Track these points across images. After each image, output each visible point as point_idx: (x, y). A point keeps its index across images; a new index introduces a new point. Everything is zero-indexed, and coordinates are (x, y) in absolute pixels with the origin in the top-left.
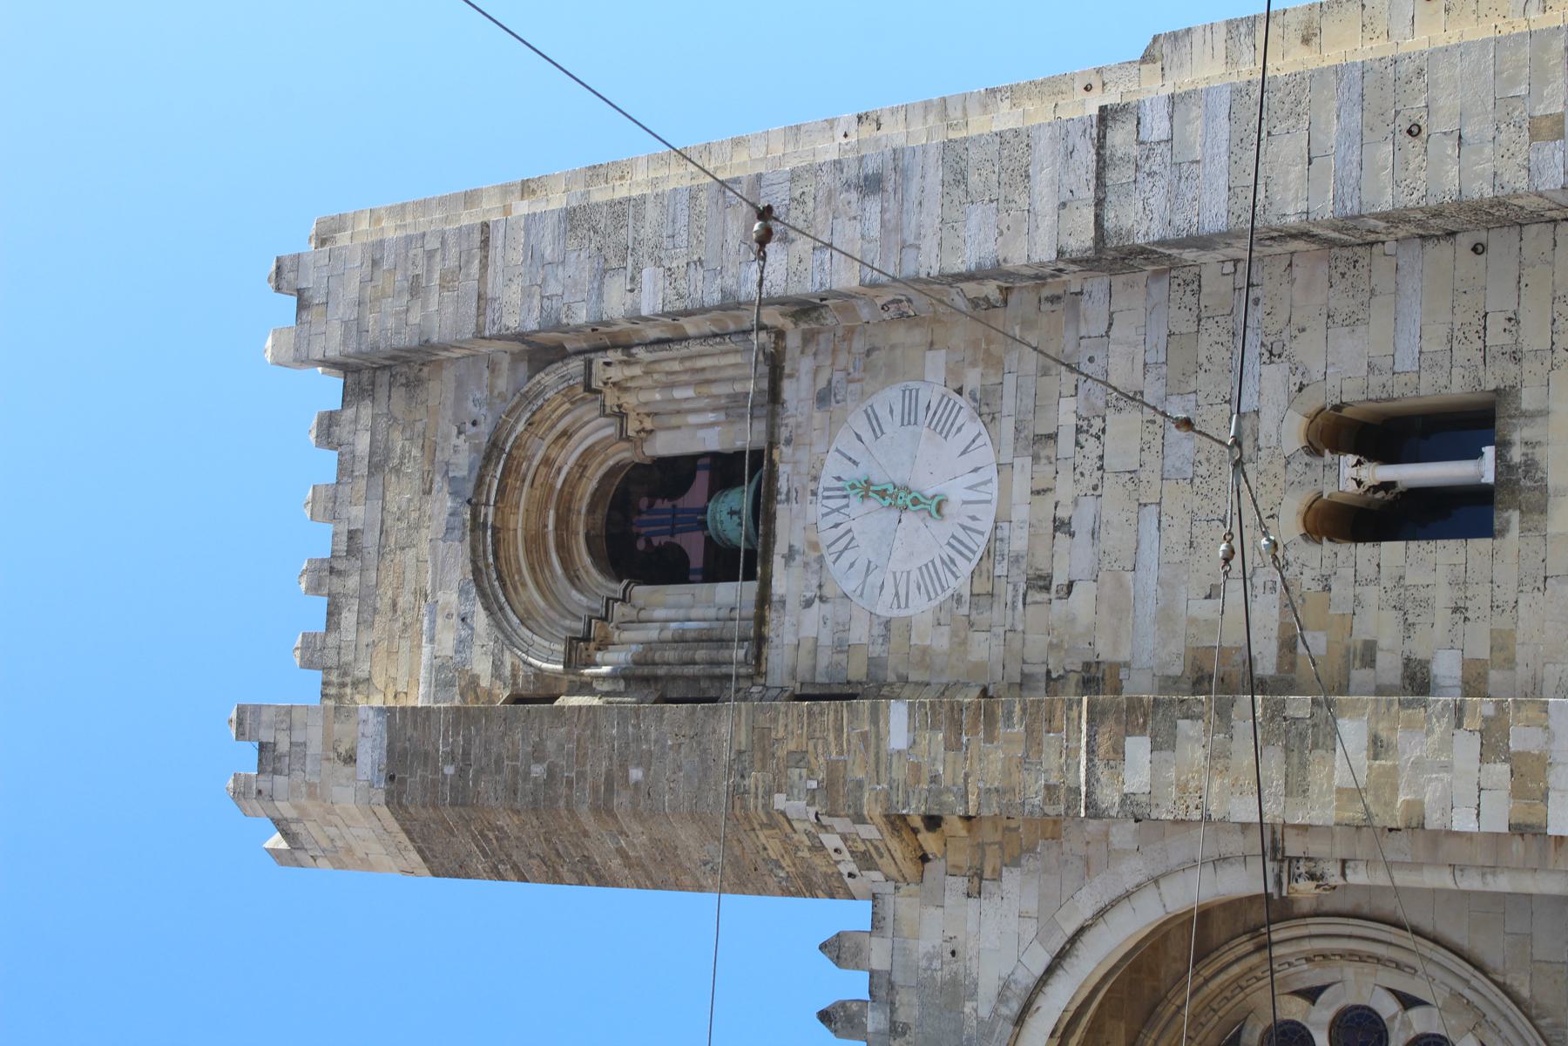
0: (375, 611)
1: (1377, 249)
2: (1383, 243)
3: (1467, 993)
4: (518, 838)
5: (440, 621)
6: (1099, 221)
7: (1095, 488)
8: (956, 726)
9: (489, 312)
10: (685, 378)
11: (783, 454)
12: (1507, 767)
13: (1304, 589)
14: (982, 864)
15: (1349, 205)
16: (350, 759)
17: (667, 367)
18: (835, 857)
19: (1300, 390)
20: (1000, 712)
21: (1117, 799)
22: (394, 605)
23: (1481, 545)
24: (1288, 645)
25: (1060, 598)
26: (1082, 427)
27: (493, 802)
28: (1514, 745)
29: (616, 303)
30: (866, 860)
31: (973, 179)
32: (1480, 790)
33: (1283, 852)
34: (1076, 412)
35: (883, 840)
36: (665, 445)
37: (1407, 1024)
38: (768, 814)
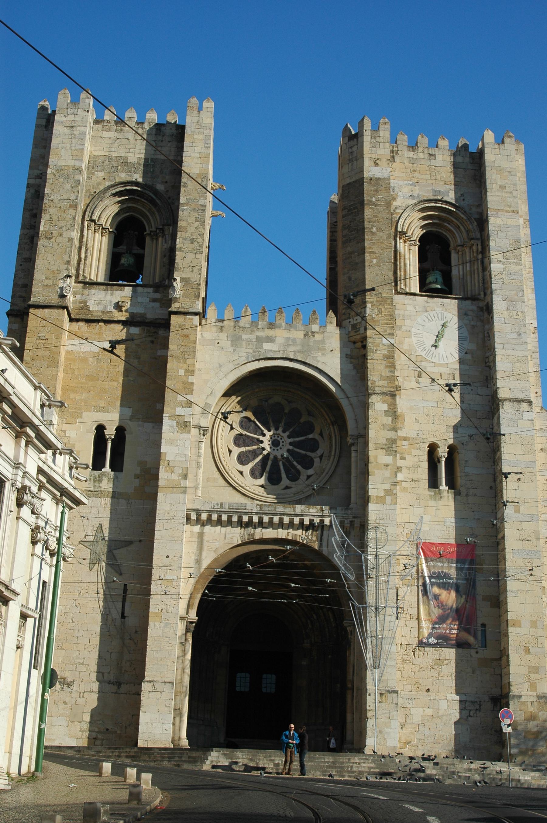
0: (413, 164)
1: (493, 464)
3: (324, 474)
4: (355, 219)
5: (411, 187)
6: (505, 400)
9: (495, 213)
10: (472, 269)
16: (376, 164)
17: (476, 264)
18: (355, 318)
19: (463, 444)
22: (415, 171)
24: (405, 439)
27: (365, 214)
28: (387, 497)
29: (495, 255)
30: (354, 327)
31: (519, 365)
36: (454, 257)
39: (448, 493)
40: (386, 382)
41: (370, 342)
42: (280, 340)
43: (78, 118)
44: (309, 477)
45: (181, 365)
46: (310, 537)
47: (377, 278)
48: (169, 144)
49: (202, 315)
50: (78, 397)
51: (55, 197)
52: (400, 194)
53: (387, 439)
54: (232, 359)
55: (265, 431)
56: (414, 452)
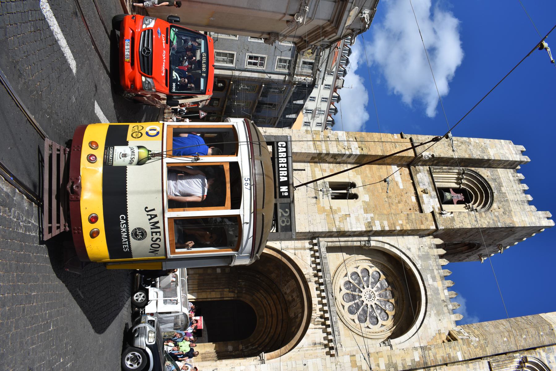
8: (449, 357)
12: (357, 365)
18: (465, 332)
37: (367, 324)
38: (479, 337)
40: (433, 358)
41: (455, 343)
42: (435, 284)
43: (515, 155)
44: (353, 320)
45: (405, 222)
46: (316, 320)
47: (497, 343)
48: (519, 208)
49: (435, 234)
50: (368, 172)
51: (471, 147)
52: (549, 354)
53: (396, 363)
54: (416, 256)
55: (375, 289)
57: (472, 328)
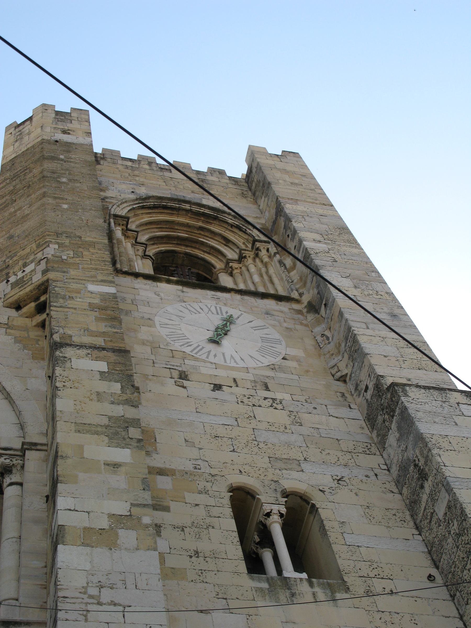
2: (420, 534)
7: (242, 402)
11: (238, 297)
13: (198, 482)
14: (16, 330)
15: (457, 483)
16: (65, 132)
20: (115, 323)
21: (66, 355)
23: (242, 567)
25: (175, 382)
26: (276, 401)
28: (121, 532)
32: (88, 513)
33: (28, 449)
34: (284, 399)
35: (32, 284)
39: (311, 585)
41: (56, 286)
53: (110, 418)
56: (191, 497)
57: (11, 262)
